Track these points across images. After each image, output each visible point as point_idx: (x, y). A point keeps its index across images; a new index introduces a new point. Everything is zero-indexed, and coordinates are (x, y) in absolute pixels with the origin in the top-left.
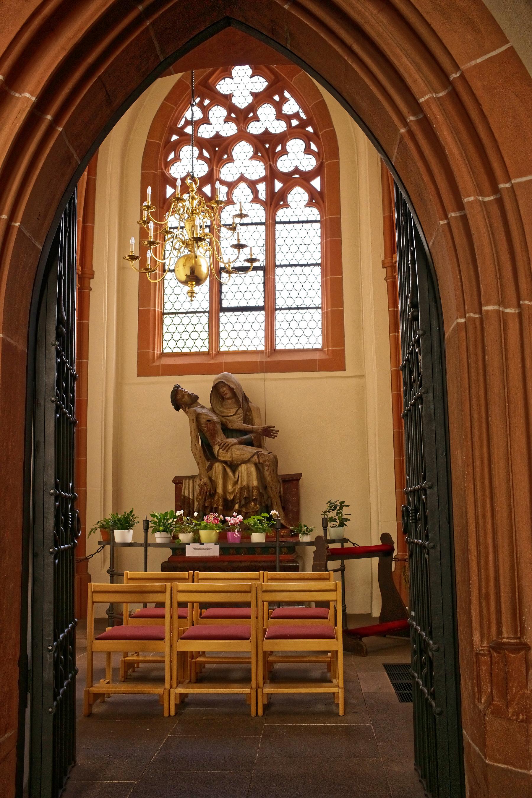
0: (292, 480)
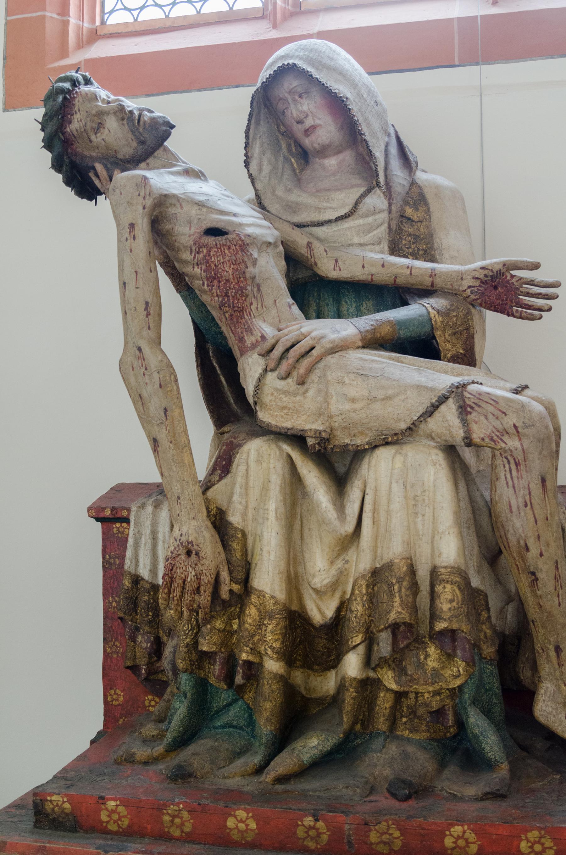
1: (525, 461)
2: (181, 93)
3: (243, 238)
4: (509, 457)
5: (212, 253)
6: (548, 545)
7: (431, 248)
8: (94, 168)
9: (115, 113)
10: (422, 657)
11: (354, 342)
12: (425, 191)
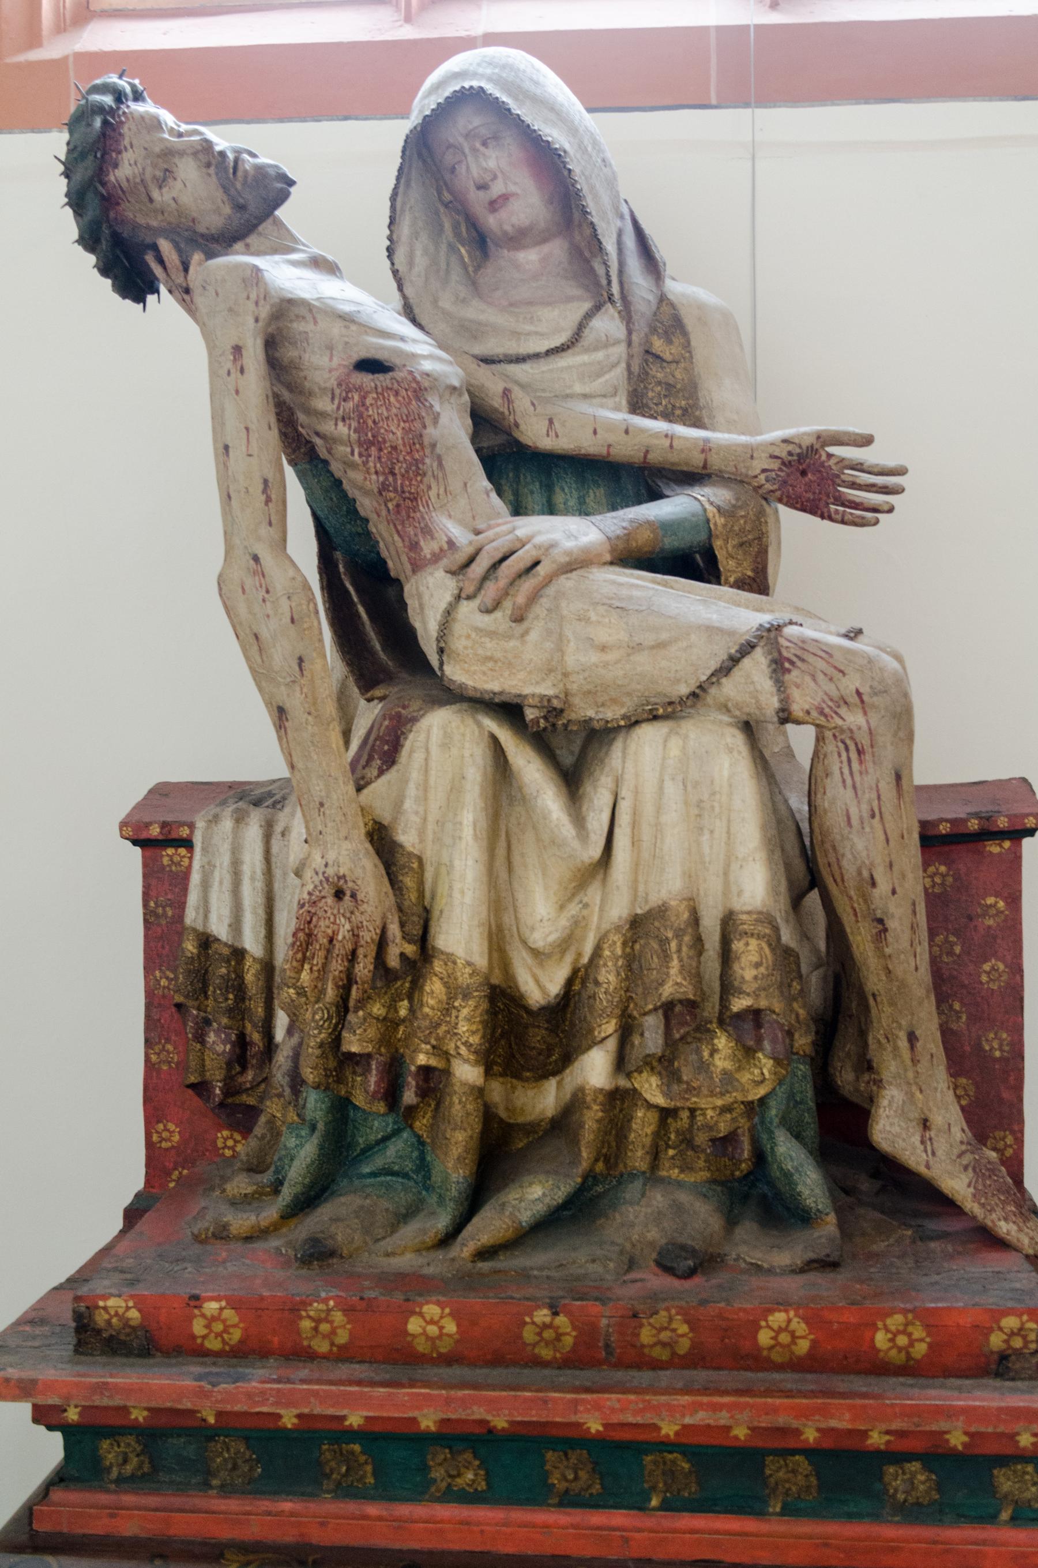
0: (988, 834)
1: (872, 746)
2: (248, 122)
3: (419, 378)
4: (848, 742)
5: (368, 402)
6: (904, 876)
7: (696, 406)
8: (155, 248)
9: (195, 154)
10: (706, 1054)
11: (600, 555)
12: (683, 312)
